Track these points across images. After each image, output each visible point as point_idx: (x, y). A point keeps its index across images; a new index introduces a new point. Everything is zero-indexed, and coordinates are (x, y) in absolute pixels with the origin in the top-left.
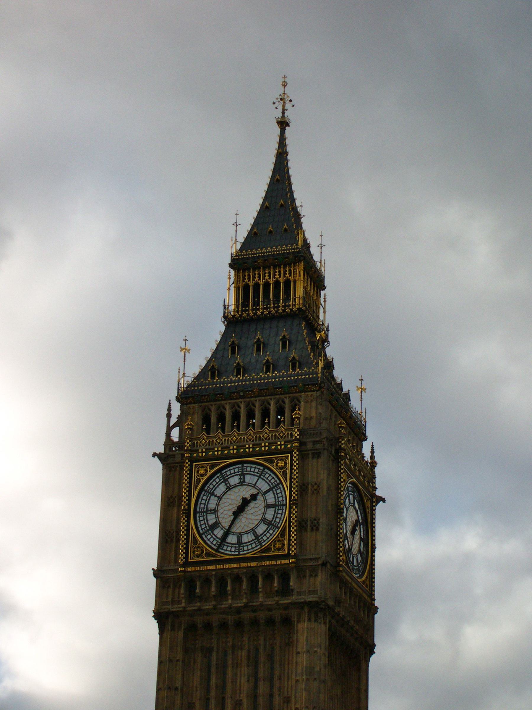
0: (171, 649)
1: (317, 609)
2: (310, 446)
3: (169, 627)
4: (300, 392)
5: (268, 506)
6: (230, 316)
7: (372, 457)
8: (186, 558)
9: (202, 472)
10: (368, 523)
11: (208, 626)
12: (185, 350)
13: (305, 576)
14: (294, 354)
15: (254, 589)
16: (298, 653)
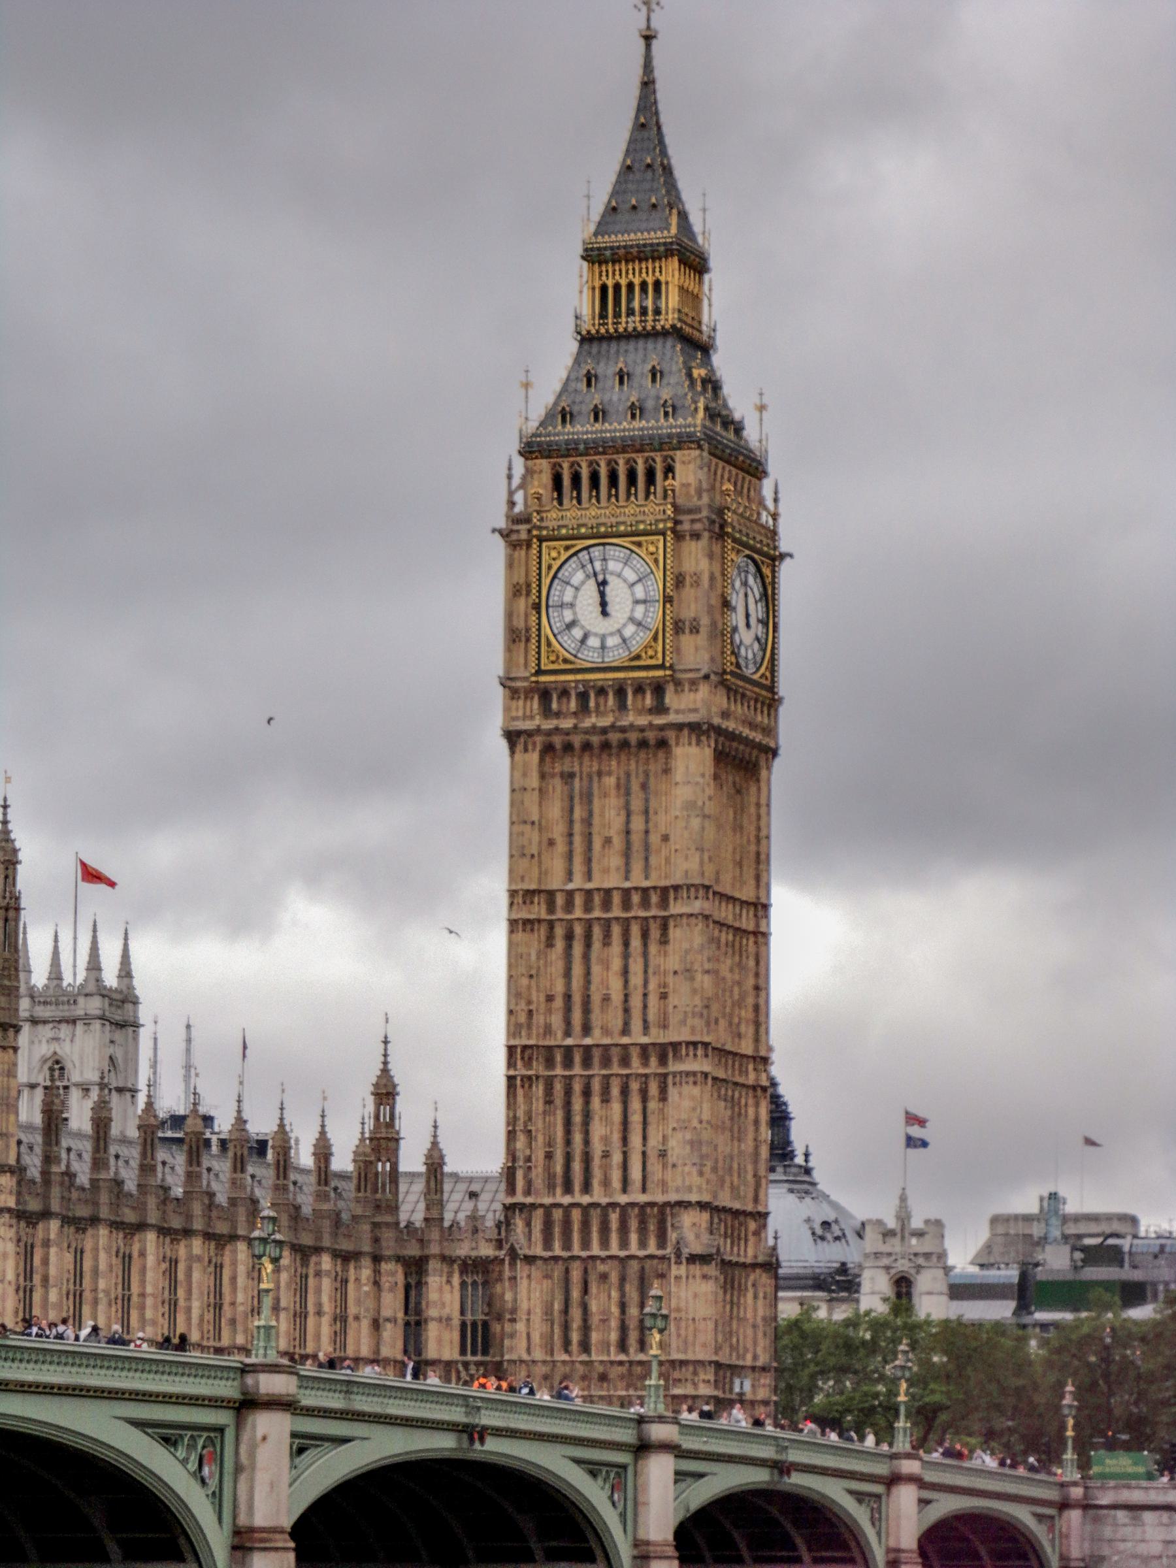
0: (525, 775)
1: (696, 729)
2: (686, 526)
3: (519, 747)
4: (675, 449)
5: (637, 602)
6: (584, 333)
7: (776, 500)
8: (539, 665)
9: (554, 554)
10: (769, 597)
11: (568, 748)
12: (527, 385)
13: (683, 691)
14: (666, 394)
15: (622, 706)
16: (677, 784)
